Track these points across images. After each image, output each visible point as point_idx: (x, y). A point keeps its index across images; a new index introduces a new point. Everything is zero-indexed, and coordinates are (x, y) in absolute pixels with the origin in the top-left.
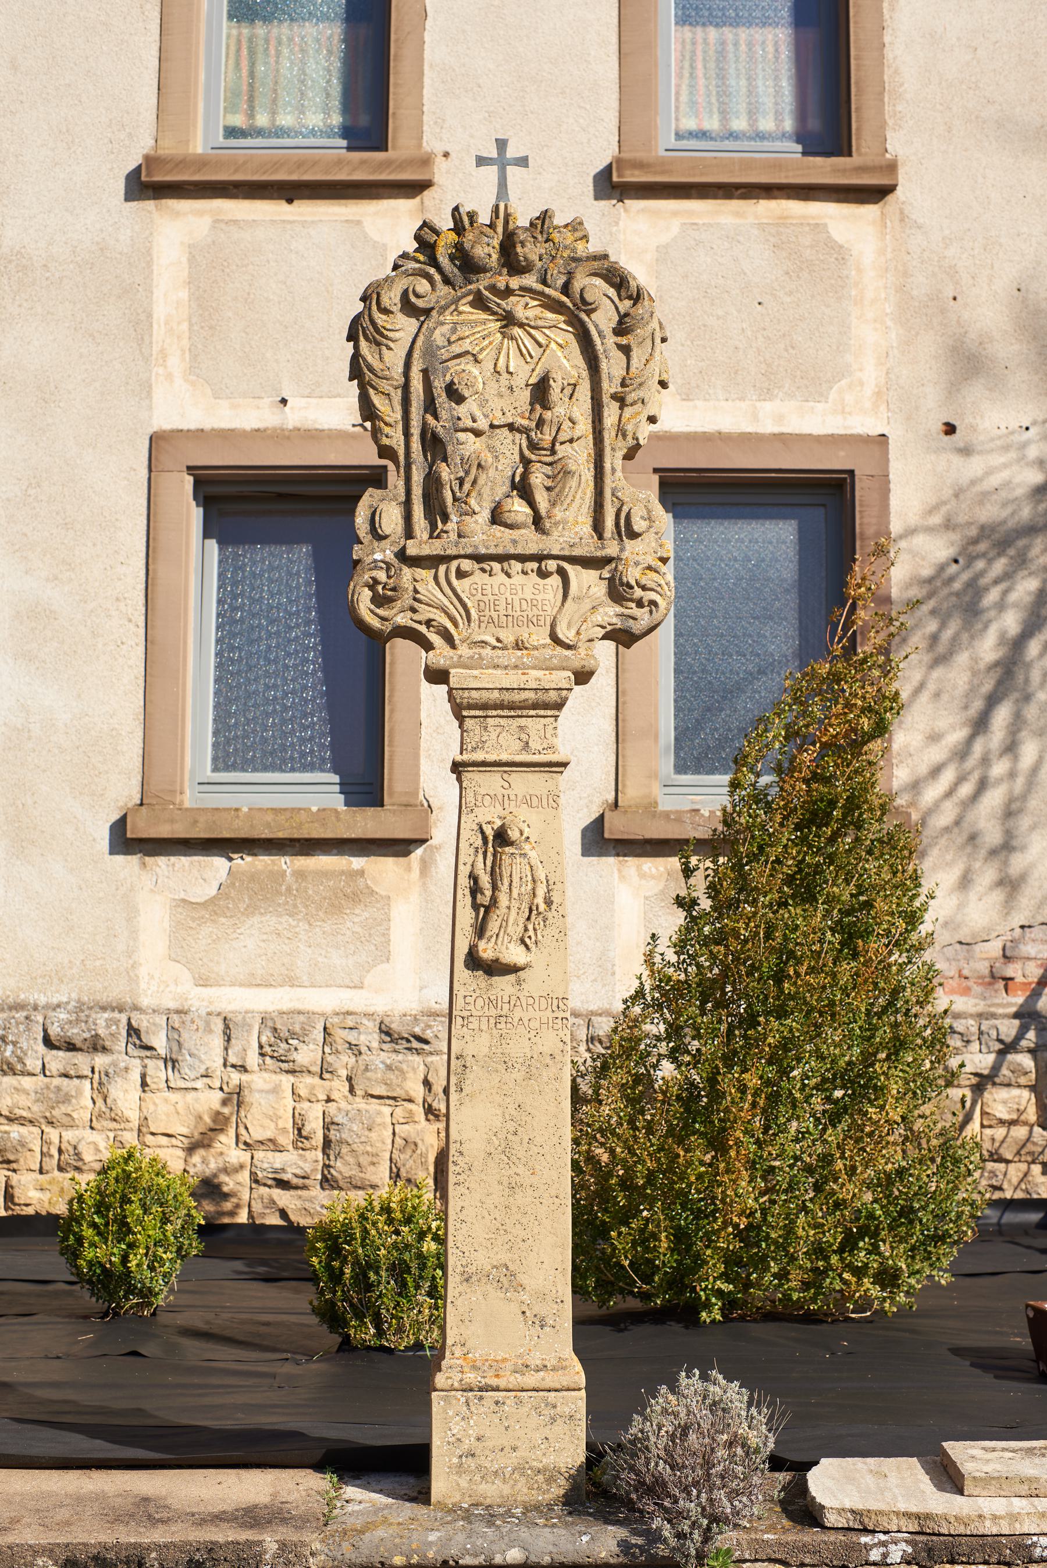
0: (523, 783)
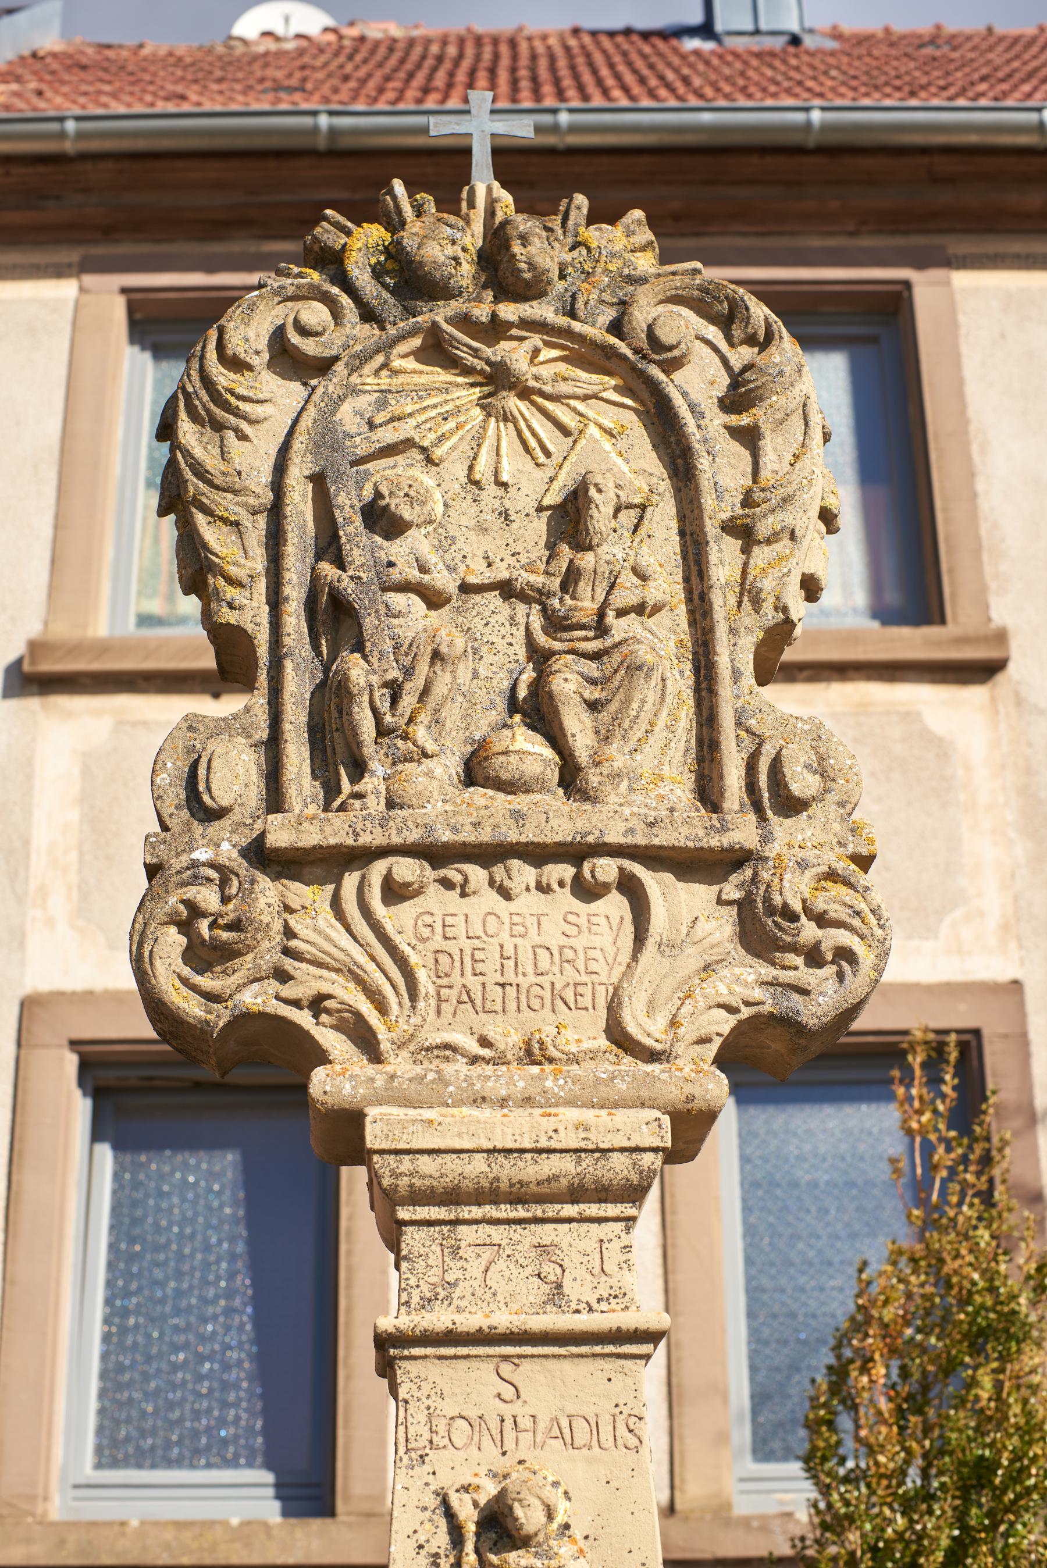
0: (553, 1385)
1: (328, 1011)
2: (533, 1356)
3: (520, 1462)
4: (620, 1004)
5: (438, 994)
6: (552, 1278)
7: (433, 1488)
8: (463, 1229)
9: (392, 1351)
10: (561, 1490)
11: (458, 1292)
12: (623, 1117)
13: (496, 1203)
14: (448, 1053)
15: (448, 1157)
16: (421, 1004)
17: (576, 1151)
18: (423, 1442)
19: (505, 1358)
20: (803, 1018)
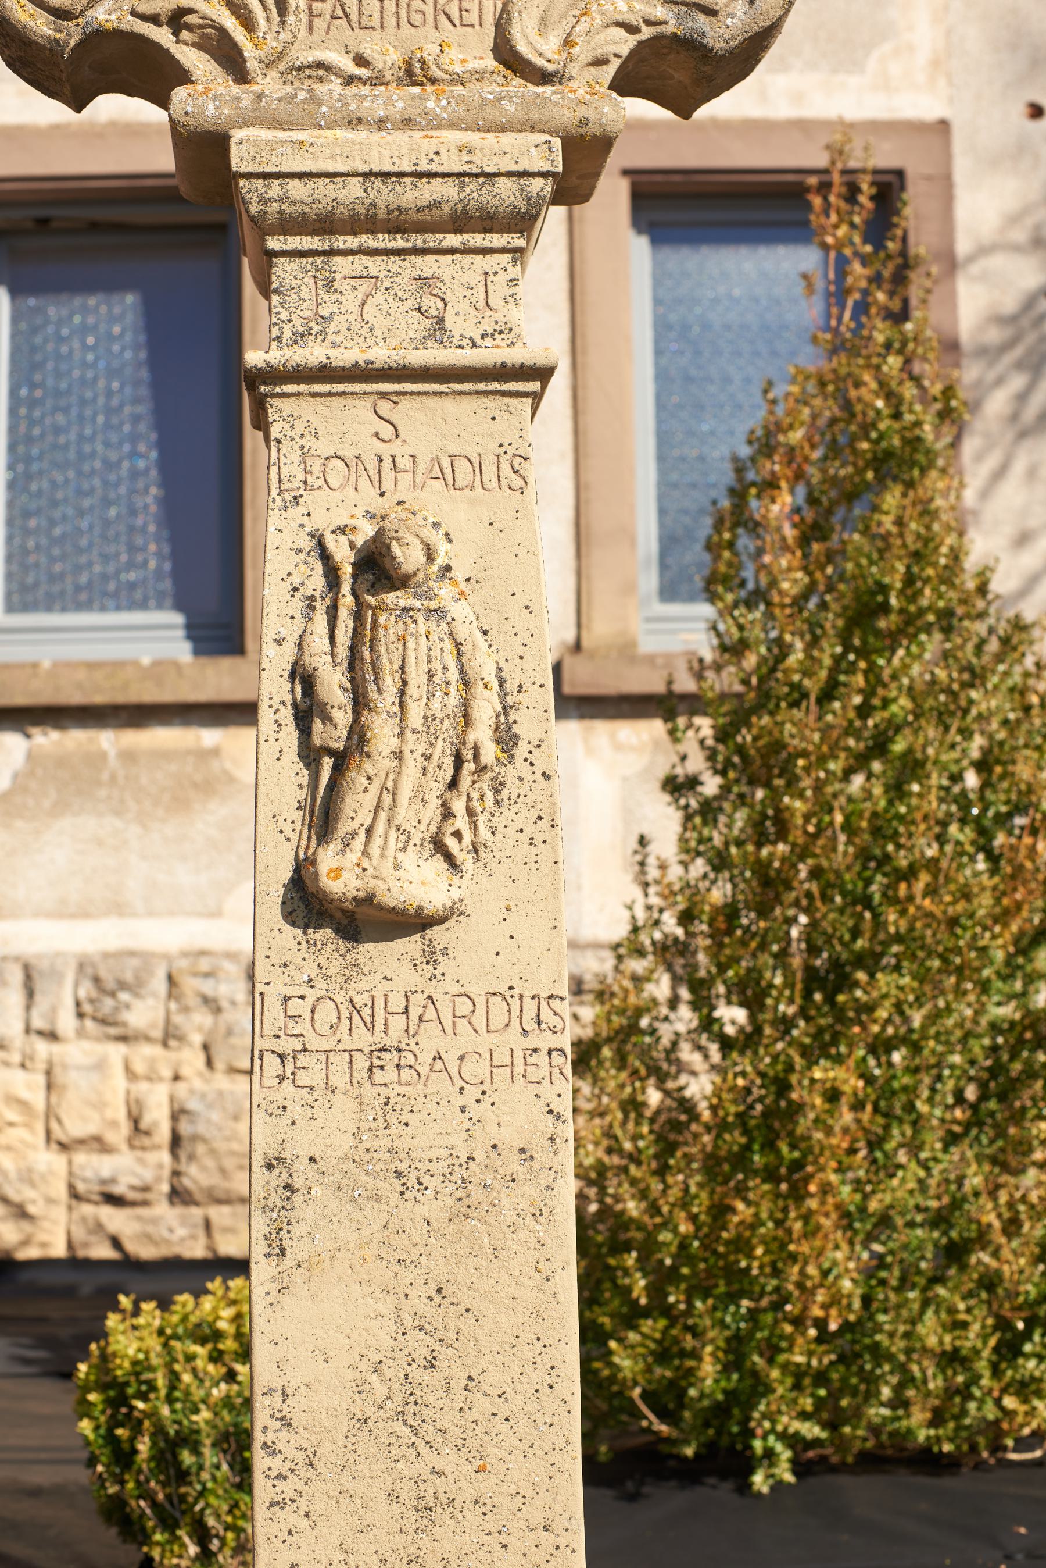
0: (433, 423)
1: (189, 28)
2: (412, 393)
3: (399, 503)
4: (509, 20)
5: (310, 8)
6: (433, 312)
7: (307, 529)
8: (337, 260)
9: (262, 389)
10: (442, 532)
11: (332, 327)
12: (508, 140)
13: (372, 232)
14: (321, 72)
15: (321, 182)
16: (291, 19)
17: (460, 175)
18: (296, 483)
19: (383, 395)
20: (709, 41)
